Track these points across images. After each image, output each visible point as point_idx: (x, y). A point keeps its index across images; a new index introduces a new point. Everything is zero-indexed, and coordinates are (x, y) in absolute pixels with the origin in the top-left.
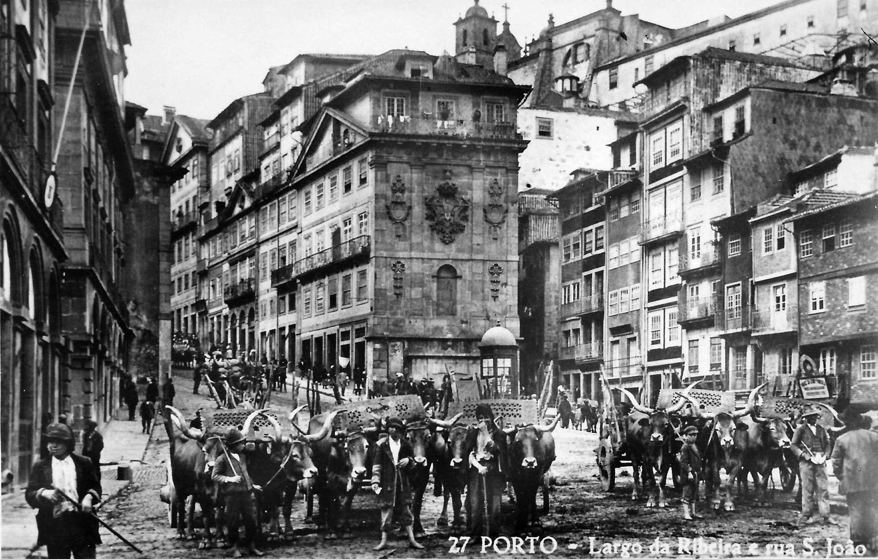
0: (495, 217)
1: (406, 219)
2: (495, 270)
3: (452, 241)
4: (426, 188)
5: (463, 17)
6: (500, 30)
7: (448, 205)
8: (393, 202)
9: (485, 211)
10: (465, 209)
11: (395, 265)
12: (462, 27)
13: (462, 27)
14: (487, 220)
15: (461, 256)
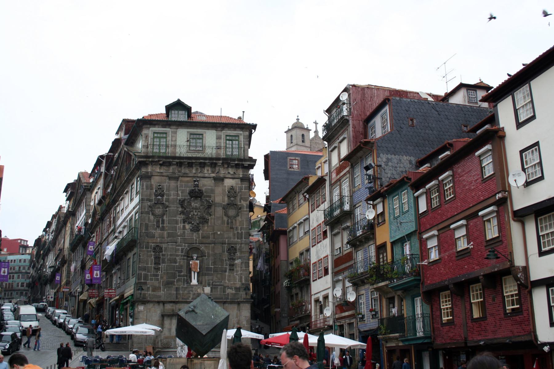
0: (232, 212)
1: (163, 215)
2: (232, 250)
3: (199, 231)
4: (180, 193)
5: (290, 128)
6: (312, 135)
7: (195, 204)
8: (155, 203)
9: (224, 208)
10: (209, 207)
11: (154, 248)
12: (290, 134)
13: (290, 134)
14: (226, 215)
15: (205, 241)
